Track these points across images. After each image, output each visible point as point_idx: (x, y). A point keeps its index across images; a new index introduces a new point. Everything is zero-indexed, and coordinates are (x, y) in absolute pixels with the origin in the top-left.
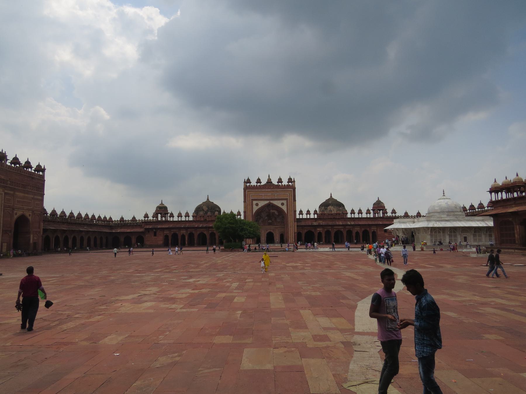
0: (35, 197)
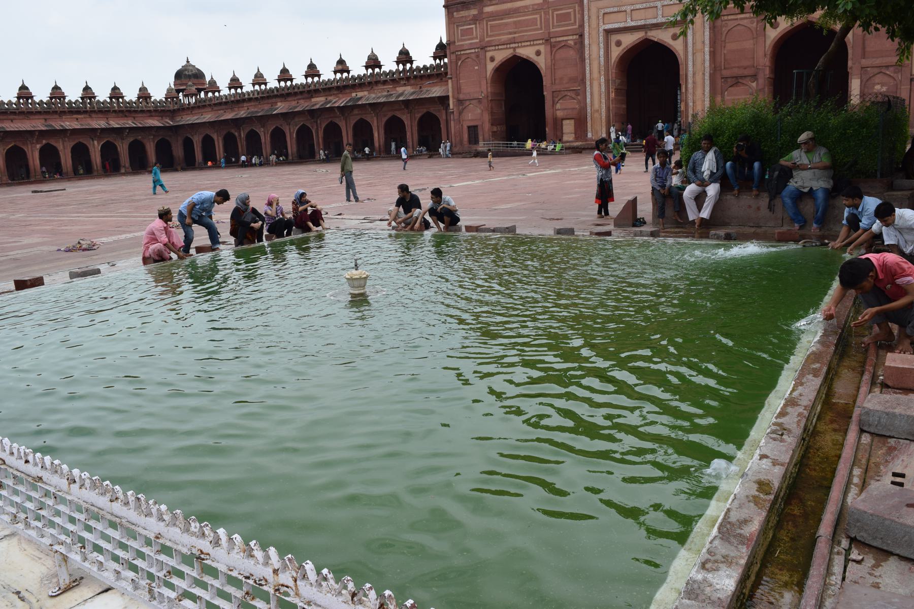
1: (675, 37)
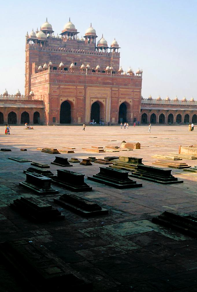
0: (134, 90)
1: (103, 101)
